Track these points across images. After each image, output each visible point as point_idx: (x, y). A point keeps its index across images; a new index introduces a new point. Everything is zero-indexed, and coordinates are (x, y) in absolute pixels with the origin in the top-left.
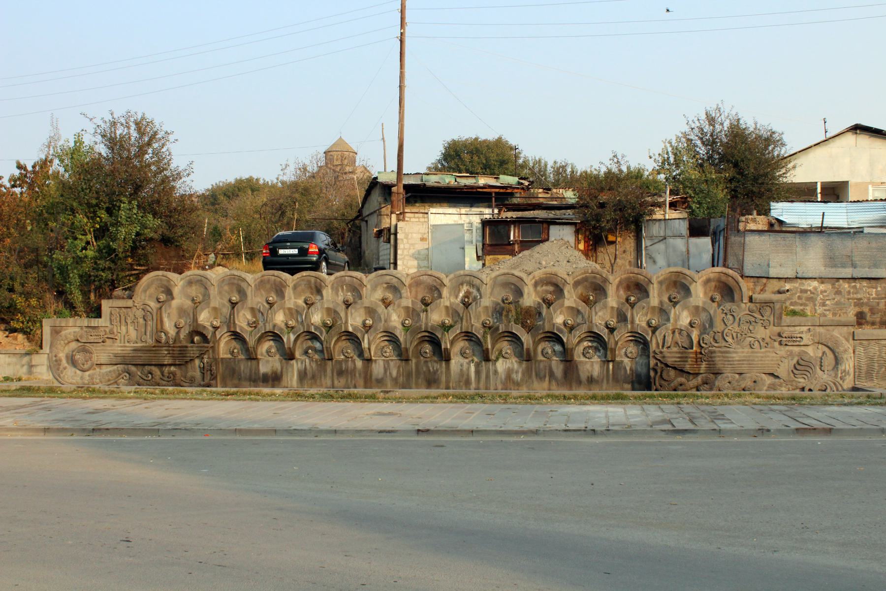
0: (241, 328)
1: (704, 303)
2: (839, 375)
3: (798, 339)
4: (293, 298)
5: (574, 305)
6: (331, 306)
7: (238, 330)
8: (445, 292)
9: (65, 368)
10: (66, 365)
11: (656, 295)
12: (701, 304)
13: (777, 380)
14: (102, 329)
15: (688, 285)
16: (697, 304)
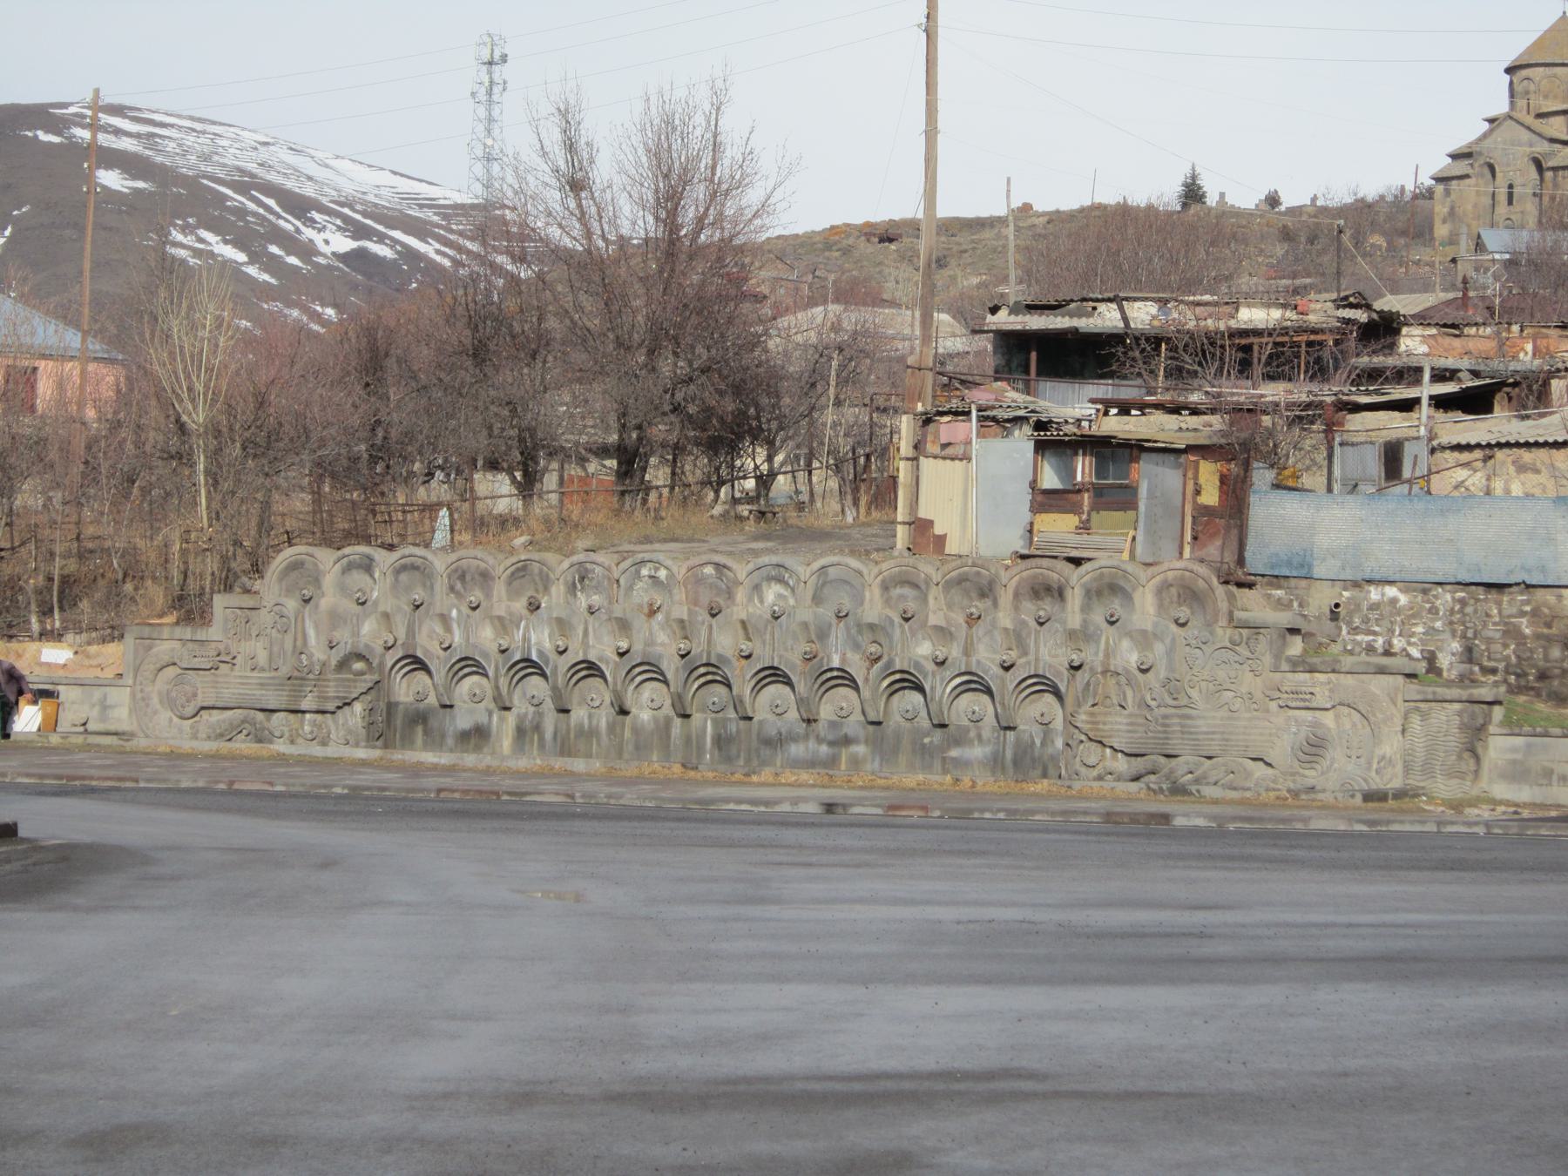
0: (426, 651)
1: (1156, 625)
2: (1375, 766)
3: (1308, 696)
4: (505, 597)
5: (943, 623)
6: (563, 615)
7: (419, 654)
8: (740, 595)
9: (155, 712)
10: (158, 706)
11: (1077, 608)
12: (1149, 627)
13: (1270, 771)
14: (213, 645)
15: (1130, 590)
16: (1143, 627)
